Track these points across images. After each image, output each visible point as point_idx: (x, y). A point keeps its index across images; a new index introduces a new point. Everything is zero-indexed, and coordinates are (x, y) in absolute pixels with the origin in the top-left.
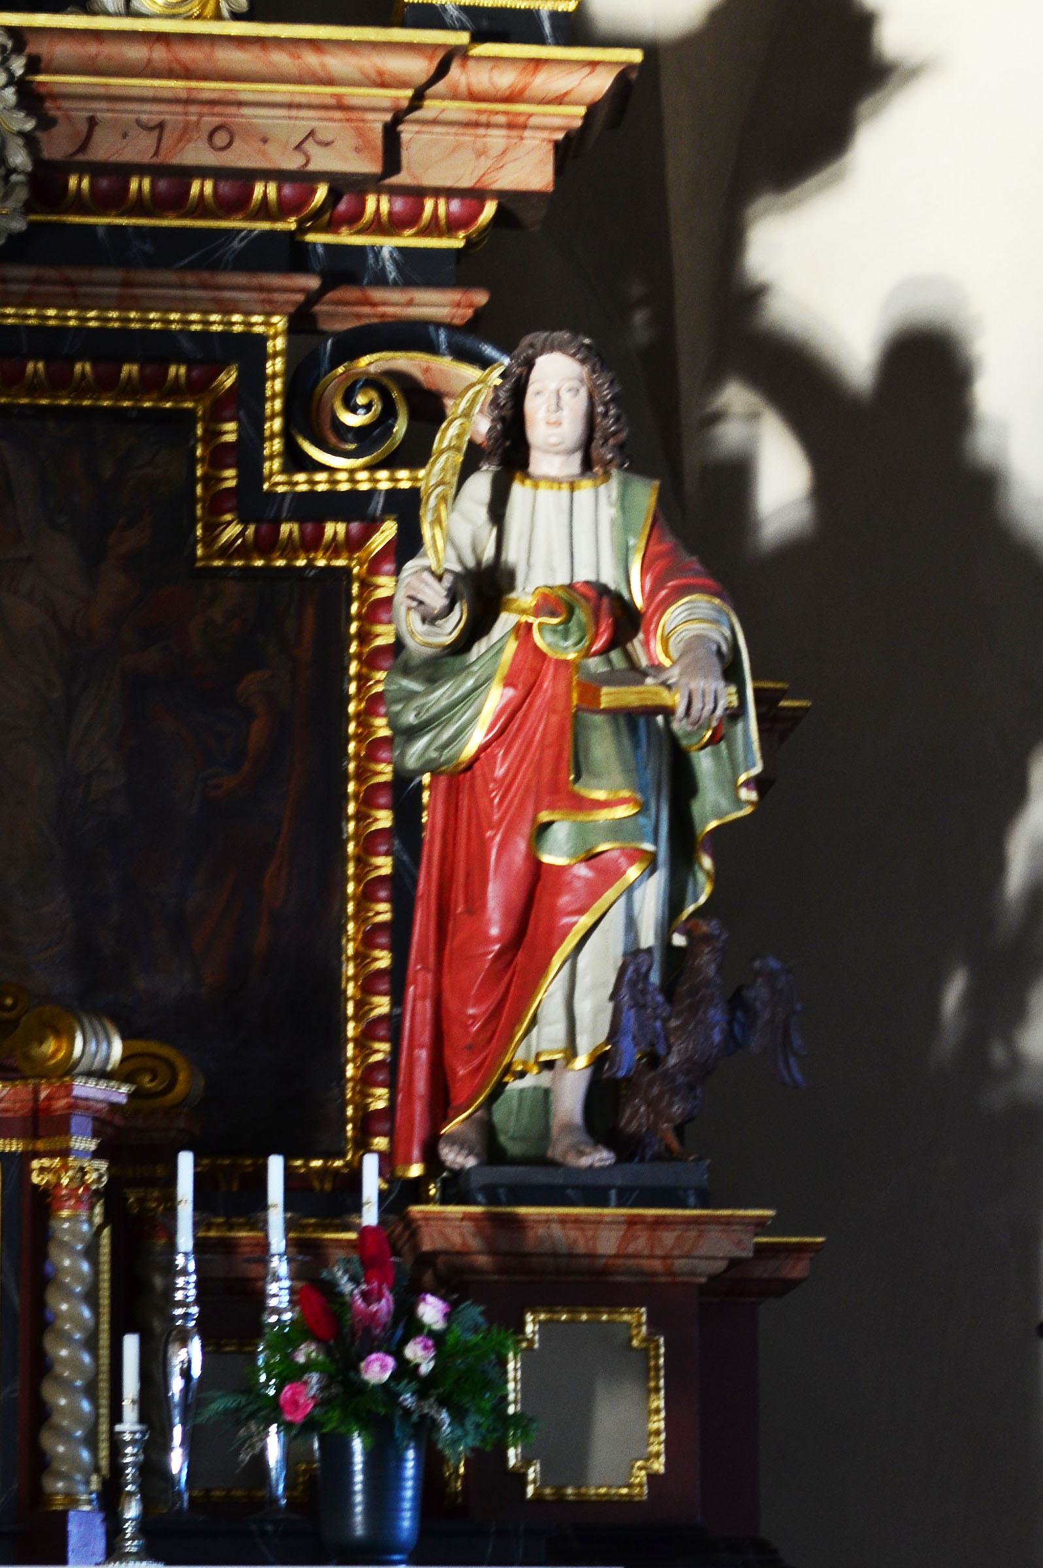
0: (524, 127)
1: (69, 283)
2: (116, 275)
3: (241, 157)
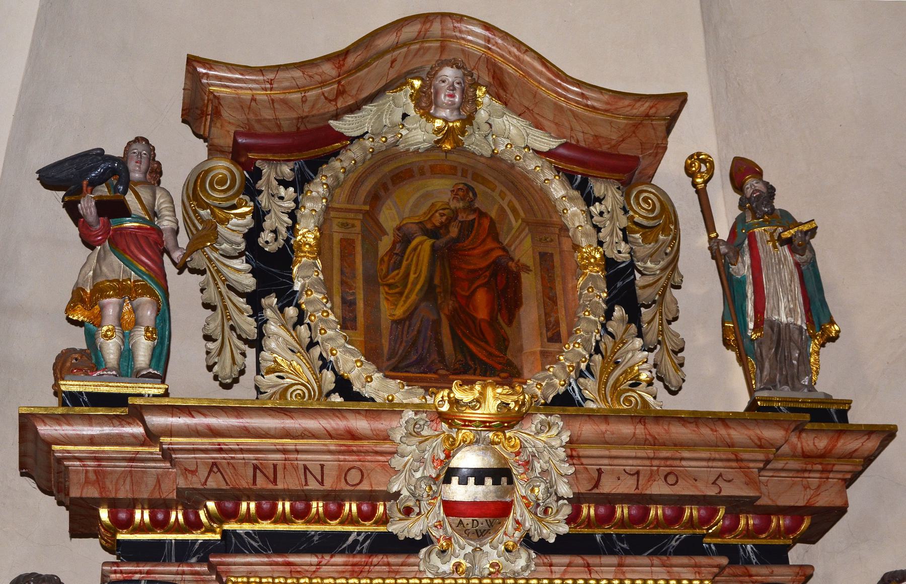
0: (831, 471)
3: (683, 489)
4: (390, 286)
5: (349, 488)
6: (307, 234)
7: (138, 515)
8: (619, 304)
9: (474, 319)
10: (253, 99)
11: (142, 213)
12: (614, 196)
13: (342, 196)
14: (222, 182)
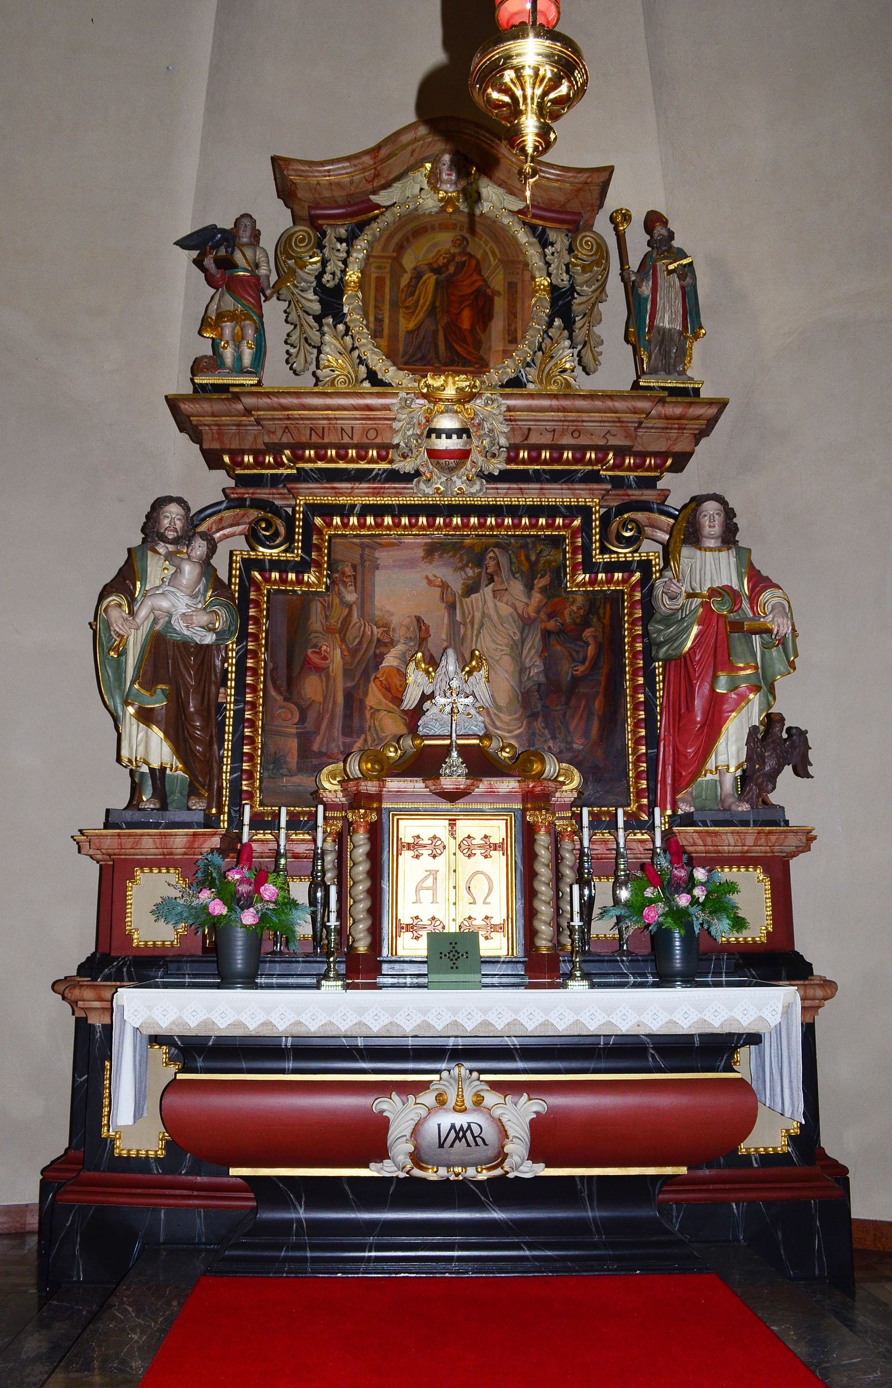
0: (685, 429)
1: (521, 489)
2: (538, 486)
3: (583, 441)
4: (407, 308)
5: (368, 441)
6: (353, 276)
7: (246, 459)
8: (558, 316)
9: (460, 329)
10: (318, 184)
11: (246, 266)
12: (562, 242)
13: (378, 247)
14: (302, 241)
